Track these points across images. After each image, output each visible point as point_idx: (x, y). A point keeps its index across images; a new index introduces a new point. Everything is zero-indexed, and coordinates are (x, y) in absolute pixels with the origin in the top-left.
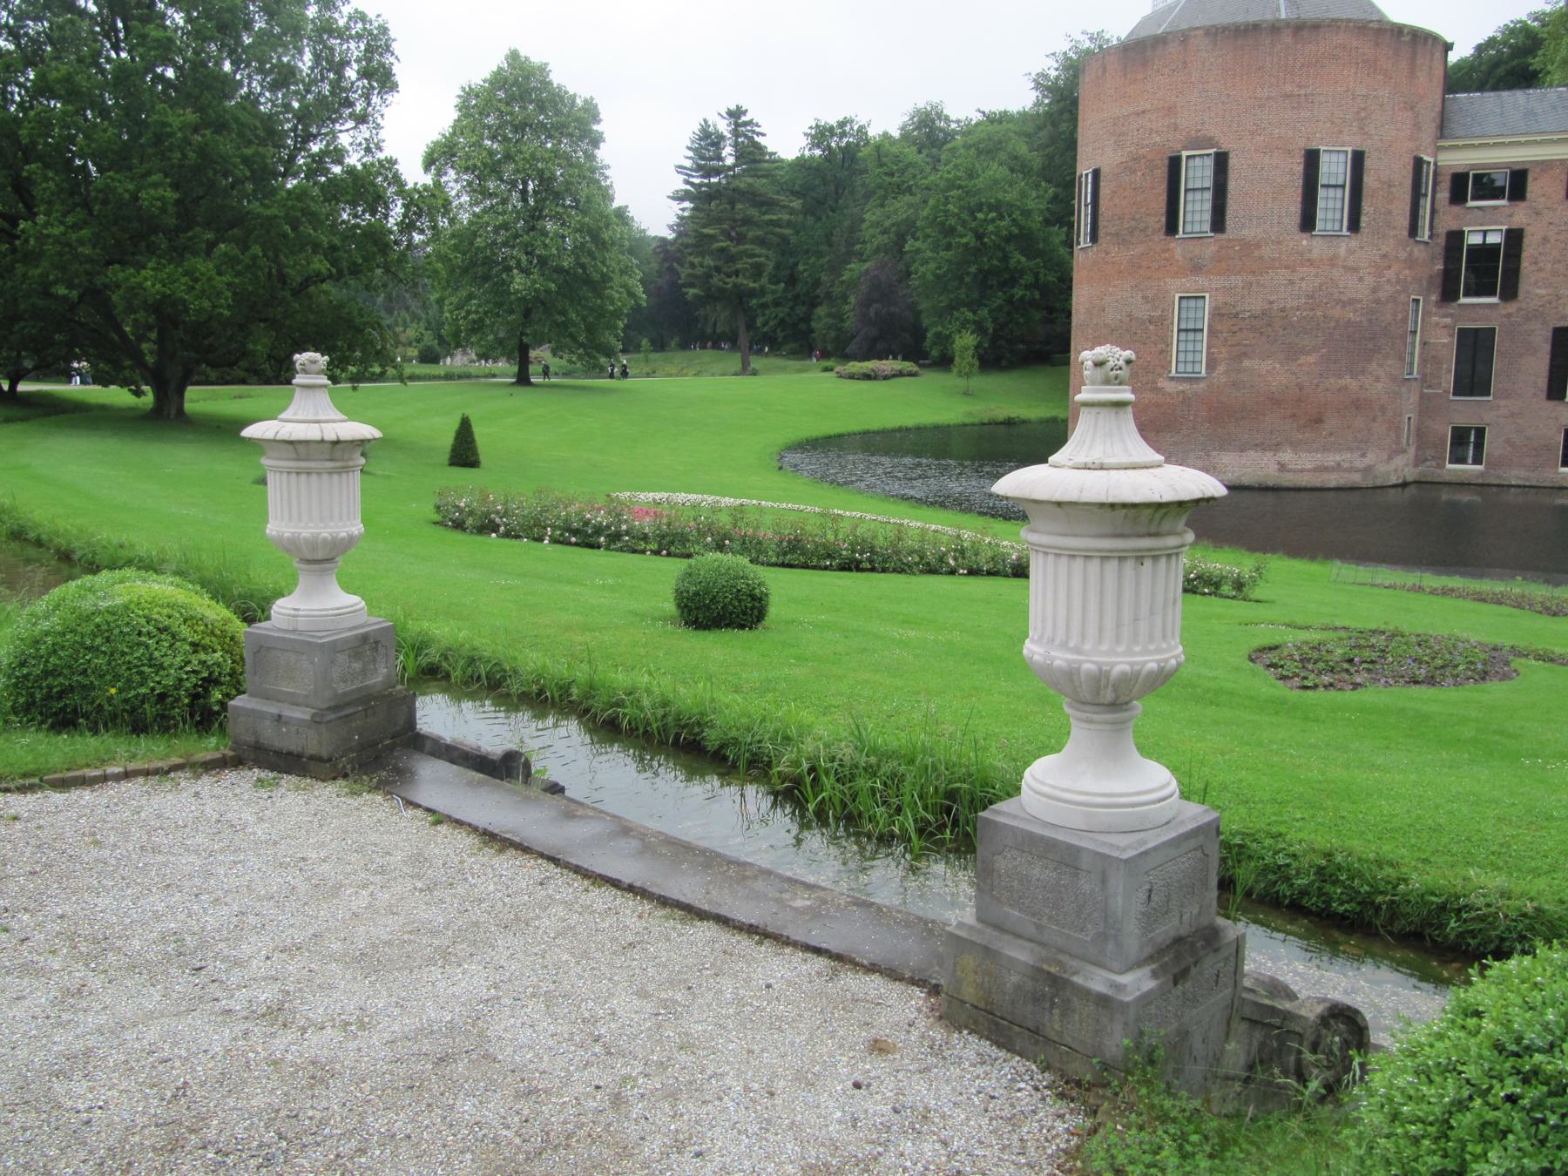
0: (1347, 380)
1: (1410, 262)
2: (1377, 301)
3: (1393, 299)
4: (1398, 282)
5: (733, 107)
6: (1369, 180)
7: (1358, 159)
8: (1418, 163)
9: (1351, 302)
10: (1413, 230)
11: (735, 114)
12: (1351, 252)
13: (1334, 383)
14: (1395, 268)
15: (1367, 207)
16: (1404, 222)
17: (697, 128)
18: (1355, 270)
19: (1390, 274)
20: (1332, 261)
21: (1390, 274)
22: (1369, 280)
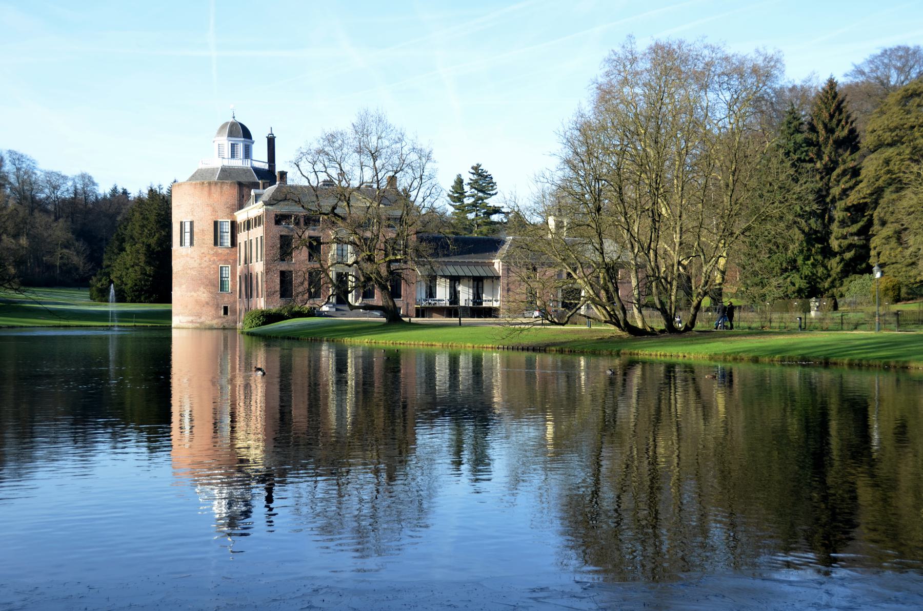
0: (193, 293)
1: (216, 254)
2: (202, 268)
3: (208, 266)
4: (210, 261)
5: (475, 165)
6: (195, 230)
7: (192, 223)
8: (216, 223)
9: (193, 268)
10: (216, 244)
11: (476, 169)
12: (192, 252)
13: (189, 294)
14: (208, 257)
15: (195, 238)
16: (213, 242)
17: (455, 178)
18: (193, 258)
19: (206, 259)
20: (187, 255)
21: (206, 259)
22: (198, 261)
